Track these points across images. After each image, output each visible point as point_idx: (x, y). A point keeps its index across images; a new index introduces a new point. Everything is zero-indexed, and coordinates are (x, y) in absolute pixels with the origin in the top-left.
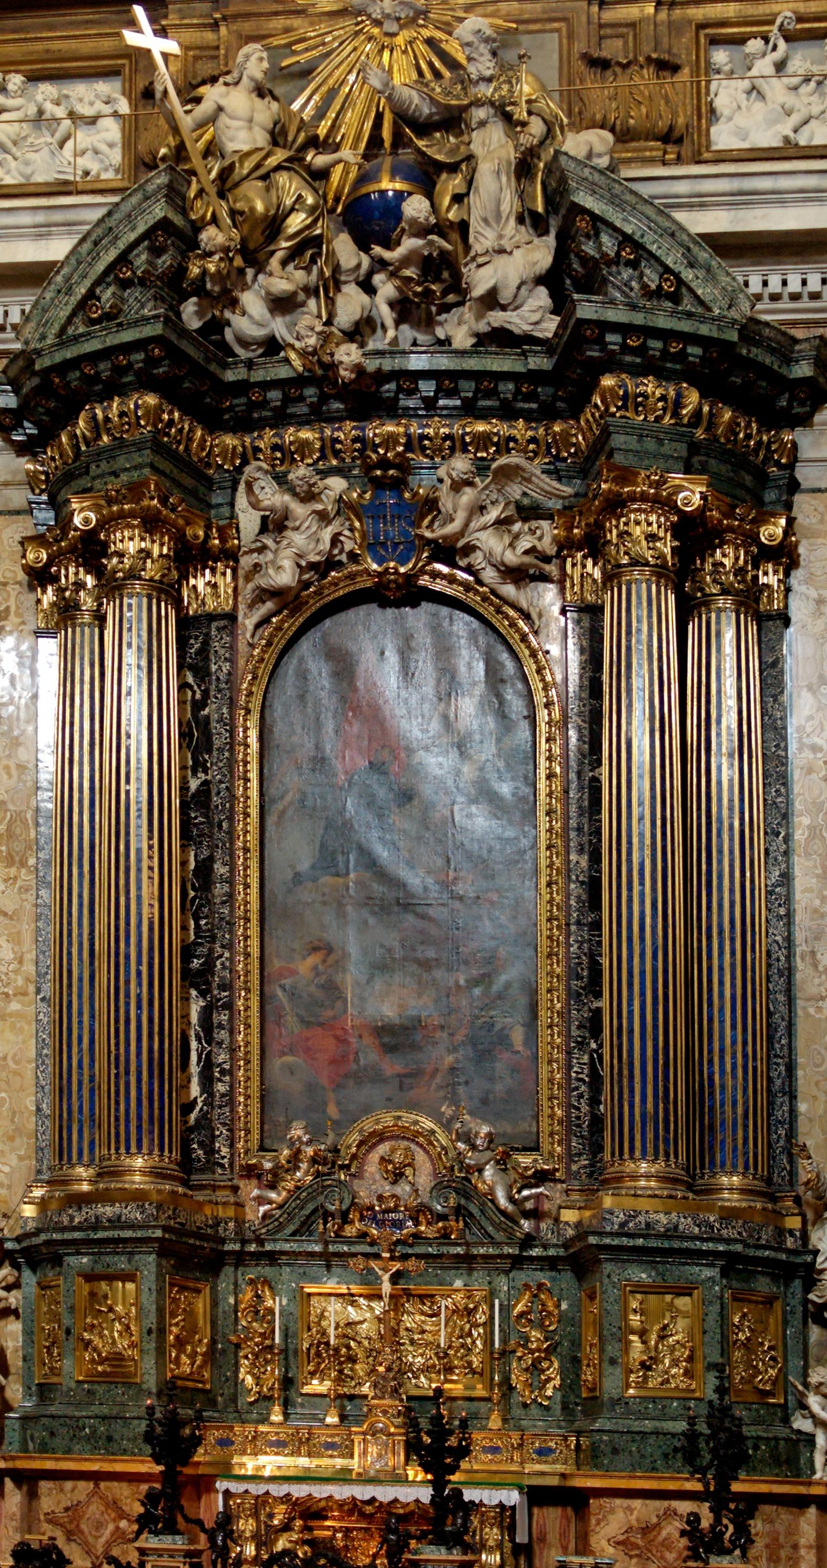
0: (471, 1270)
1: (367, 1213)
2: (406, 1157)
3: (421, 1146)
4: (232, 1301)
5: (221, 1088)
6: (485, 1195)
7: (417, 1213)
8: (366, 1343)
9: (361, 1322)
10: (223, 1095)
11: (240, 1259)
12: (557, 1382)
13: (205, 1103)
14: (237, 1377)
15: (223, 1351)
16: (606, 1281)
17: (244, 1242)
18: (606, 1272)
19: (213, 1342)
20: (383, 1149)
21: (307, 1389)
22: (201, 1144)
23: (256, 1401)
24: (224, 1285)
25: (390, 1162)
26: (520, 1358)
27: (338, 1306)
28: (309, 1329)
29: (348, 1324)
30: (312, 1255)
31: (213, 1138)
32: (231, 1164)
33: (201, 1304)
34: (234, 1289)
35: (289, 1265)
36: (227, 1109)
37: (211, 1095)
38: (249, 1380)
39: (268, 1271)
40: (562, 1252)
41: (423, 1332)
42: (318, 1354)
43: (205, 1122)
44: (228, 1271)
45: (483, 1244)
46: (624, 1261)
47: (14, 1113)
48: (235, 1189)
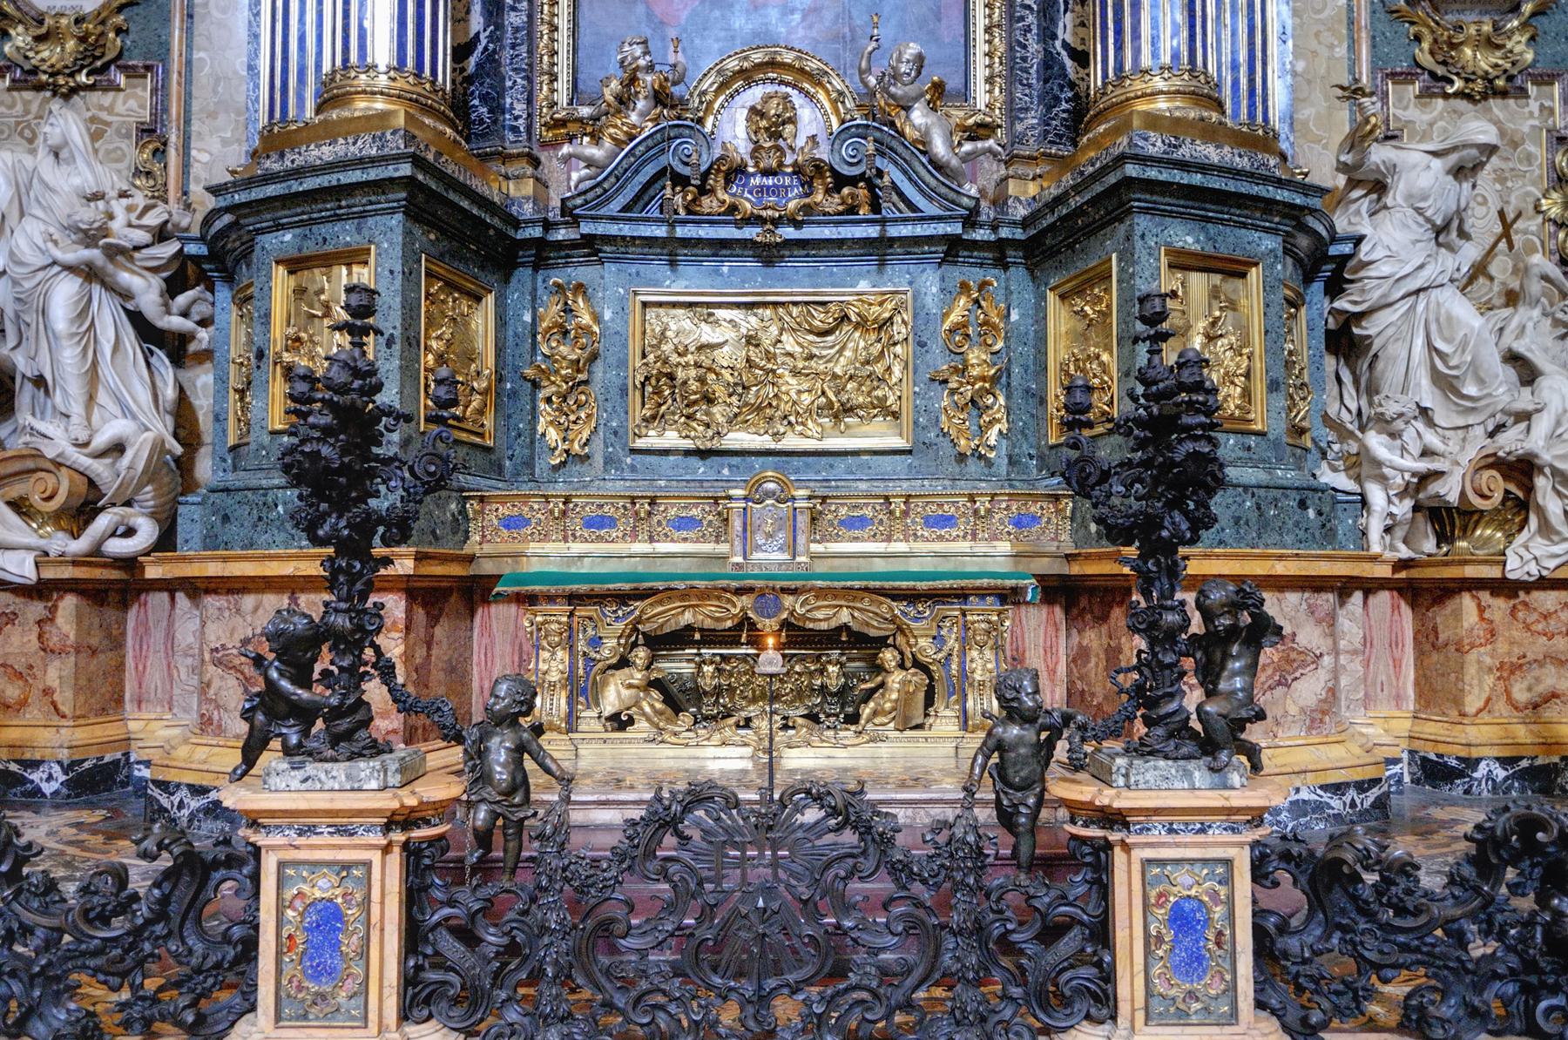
0: (882, 264)
1: (735, 172)
2: (785, 109)
3: (807, 94)
4: (527, 318)
5: (514, 19)
6: (914, 142)
7: (811, 172)
8: (726, 374)
9: (720, 345)
10: (517, 30)
11: (544, 254)
12: (1004, 426)
13: (491, 38)
14: (534, 429)
15: (514, 394)
16: (1139, 244)
17: (548, 225)
18: (1138, 231)
19: (500, 379)
20: (755, 94)
21: (640, 443)
22: (484, 99)
23: (563, 464)
24: (516, 296)
25: (762, 115)
26: (953, 392)
27: (687, 324)
28: (644, 356)
29: (700, 348)
30: (650, 241)
31: (501, 93)
32: (529, 128)
33: (482, 320)
34: (534, 300)
35: (616, 260)
36: (524, 48)
37: (499, 27)
38: (553, 435)
39: (583, 273)
40: (1019, 234)
41: (811, 357)
42: (658, 392)
43: (491, 58)
44: (523, 274)
45: (905, 220)
46: (1166, 214)
47: (218, 80)
48: (535, 162)
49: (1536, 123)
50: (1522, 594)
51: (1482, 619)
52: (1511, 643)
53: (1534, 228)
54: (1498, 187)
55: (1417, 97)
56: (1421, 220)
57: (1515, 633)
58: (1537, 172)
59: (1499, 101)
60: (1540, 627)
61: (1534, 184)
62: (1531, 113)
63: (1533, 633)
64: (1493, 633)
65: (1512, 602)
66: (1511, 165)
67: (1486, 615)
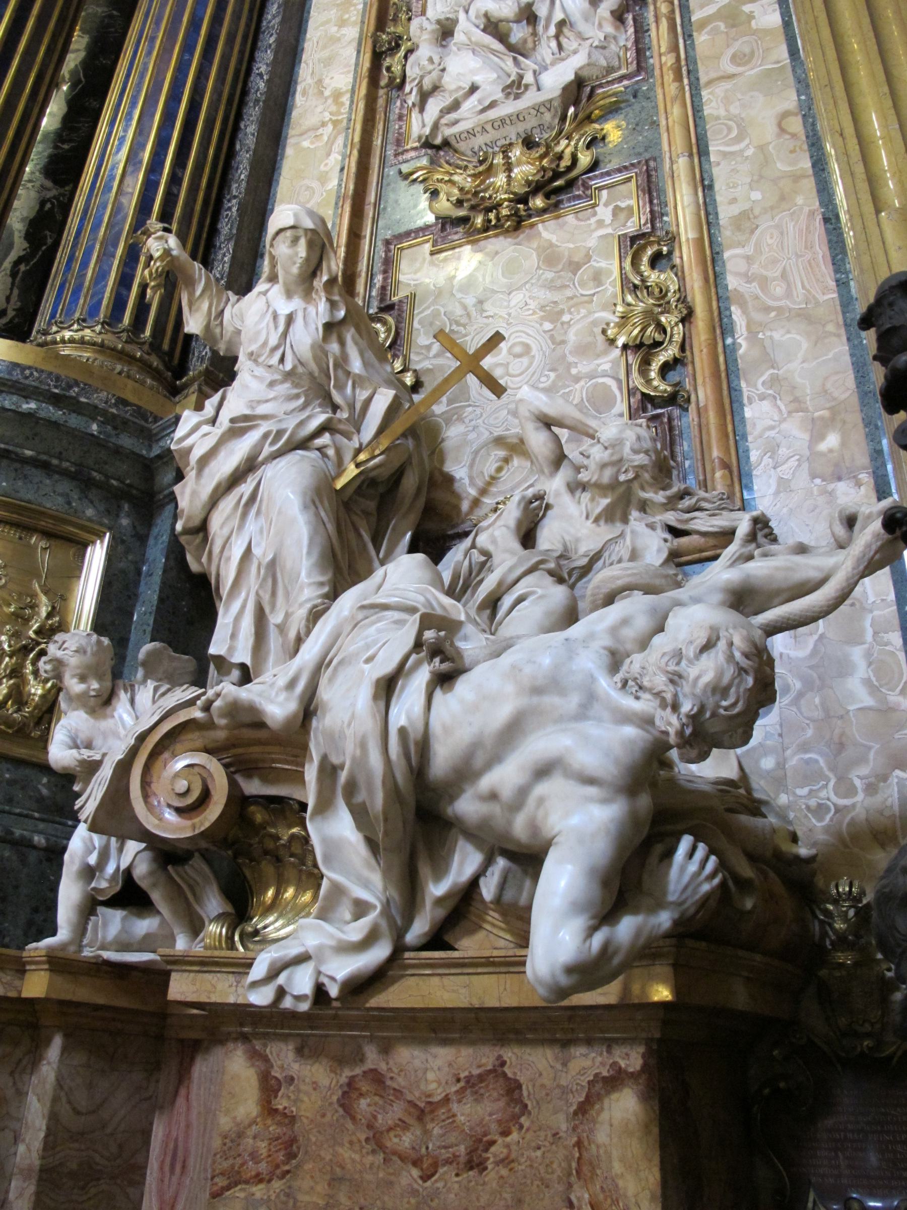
49: (609, 230)
50: (371, 1054)
51: (269, 1110)
52: (335, 1181)
53: (607, 367)
54: (548, 326)
55: (432, 253)
56: (260, 371)
57: (347, 1154)
58: (611, 289)
59: (552, 224)
60: (405, 1141)
61: (604, 308)
62: (600, 224)
63: (391, 1155)
64: (290, 1147)
65: (347, 1073)
66: (569, 293)
67: (281, 1103)
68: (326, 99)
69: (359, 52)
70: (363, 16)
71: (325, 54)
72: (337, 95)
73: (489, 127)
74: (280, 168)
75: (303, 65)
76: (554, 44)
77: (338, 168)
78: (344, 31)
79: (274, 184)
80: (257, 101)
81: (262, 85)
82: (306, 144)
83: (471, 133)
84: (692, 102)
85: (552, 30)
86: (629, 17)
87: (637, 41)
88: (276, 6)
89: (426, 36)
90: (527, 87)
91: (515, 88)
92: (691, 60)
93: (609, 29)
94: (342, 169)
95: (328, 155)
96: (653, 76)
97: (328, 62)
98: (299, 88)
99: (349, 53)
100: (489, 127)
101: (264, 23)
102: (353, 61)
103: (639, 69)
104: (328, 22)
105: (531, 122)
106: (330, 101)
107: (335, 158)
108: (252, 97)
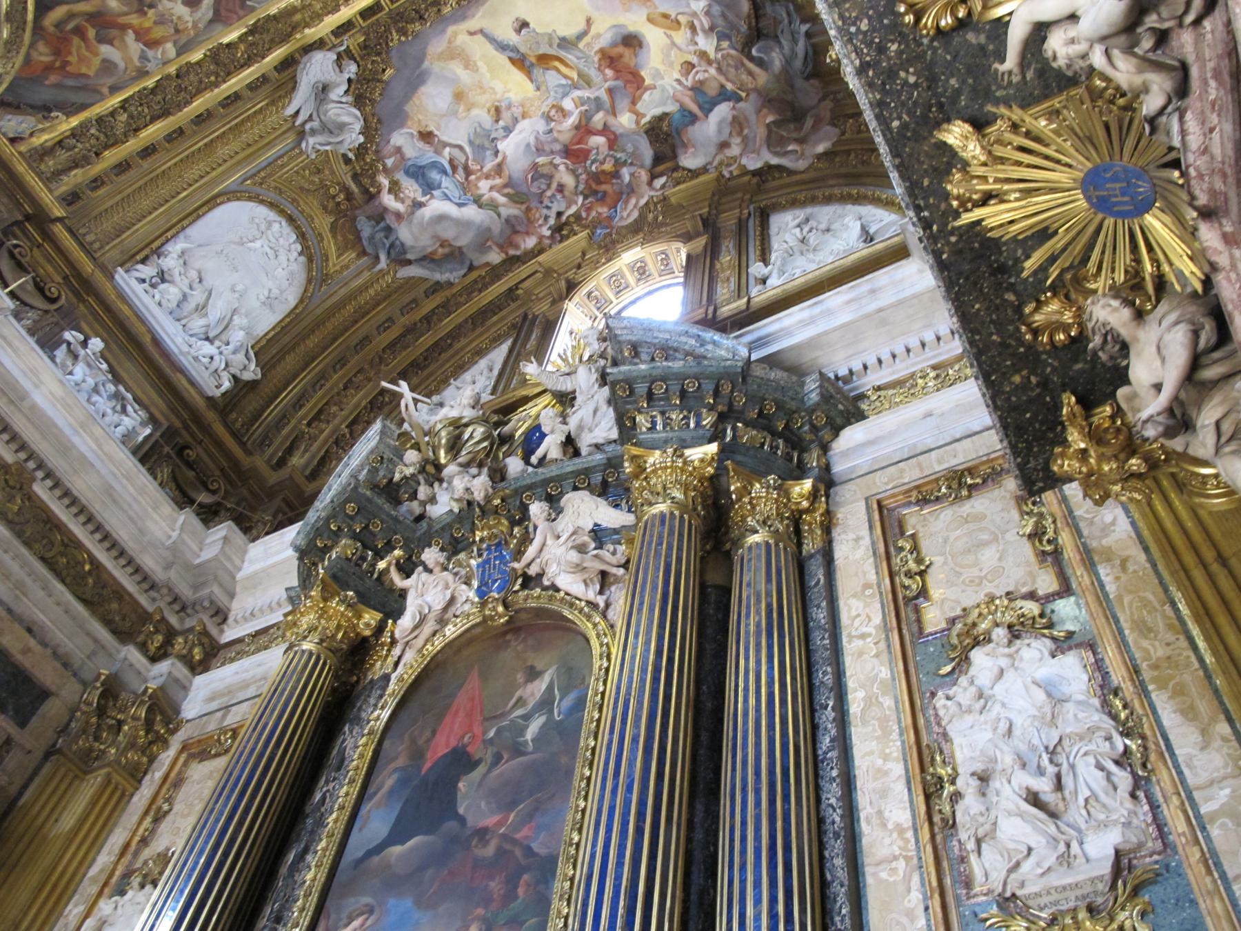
68: (891, 831)
69: (909, 789)
70: (904, 754)
71: (877, 785)
72: (900, 830)
73: (1053, 891)
74: (865, 895)
75: (859, 793)
76: (1084, 812)
77: (922, 908)
78: (890, 765)
79: (864, 912)
80: (837, 835)
81: (838, 819)
82: (884, 875)
83: (1038, 895)
84: (1228, 895)
85: (1081, 801)
86: (1141, 794)
87: (1155, 818)
88: (828, 740)
89: (970, 790)
90: (1075, 857)
91: (1066, 859)
92: (1214, 853)
93: (1129, 804)
94: (927, 909)
95: (909, 891)
96: (1176, 853)
97: (884, 793)
98: (862, 815)
99: (901, 787)
100: (1053, 891)
101: (820, 752)
102: (906, 797)
103: (1165, 845)
104: (871, 753)
105: (1088, 889)
106: (895, 835)
107: (915, 897)
108: (828, 827)
